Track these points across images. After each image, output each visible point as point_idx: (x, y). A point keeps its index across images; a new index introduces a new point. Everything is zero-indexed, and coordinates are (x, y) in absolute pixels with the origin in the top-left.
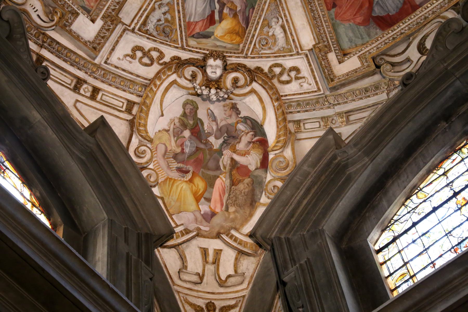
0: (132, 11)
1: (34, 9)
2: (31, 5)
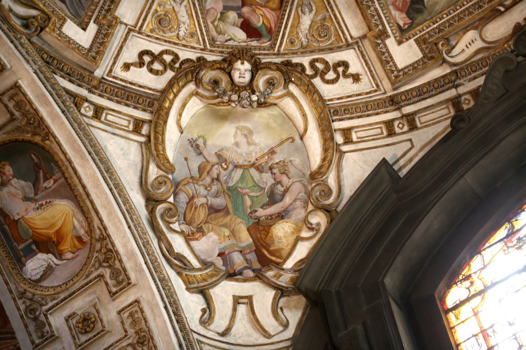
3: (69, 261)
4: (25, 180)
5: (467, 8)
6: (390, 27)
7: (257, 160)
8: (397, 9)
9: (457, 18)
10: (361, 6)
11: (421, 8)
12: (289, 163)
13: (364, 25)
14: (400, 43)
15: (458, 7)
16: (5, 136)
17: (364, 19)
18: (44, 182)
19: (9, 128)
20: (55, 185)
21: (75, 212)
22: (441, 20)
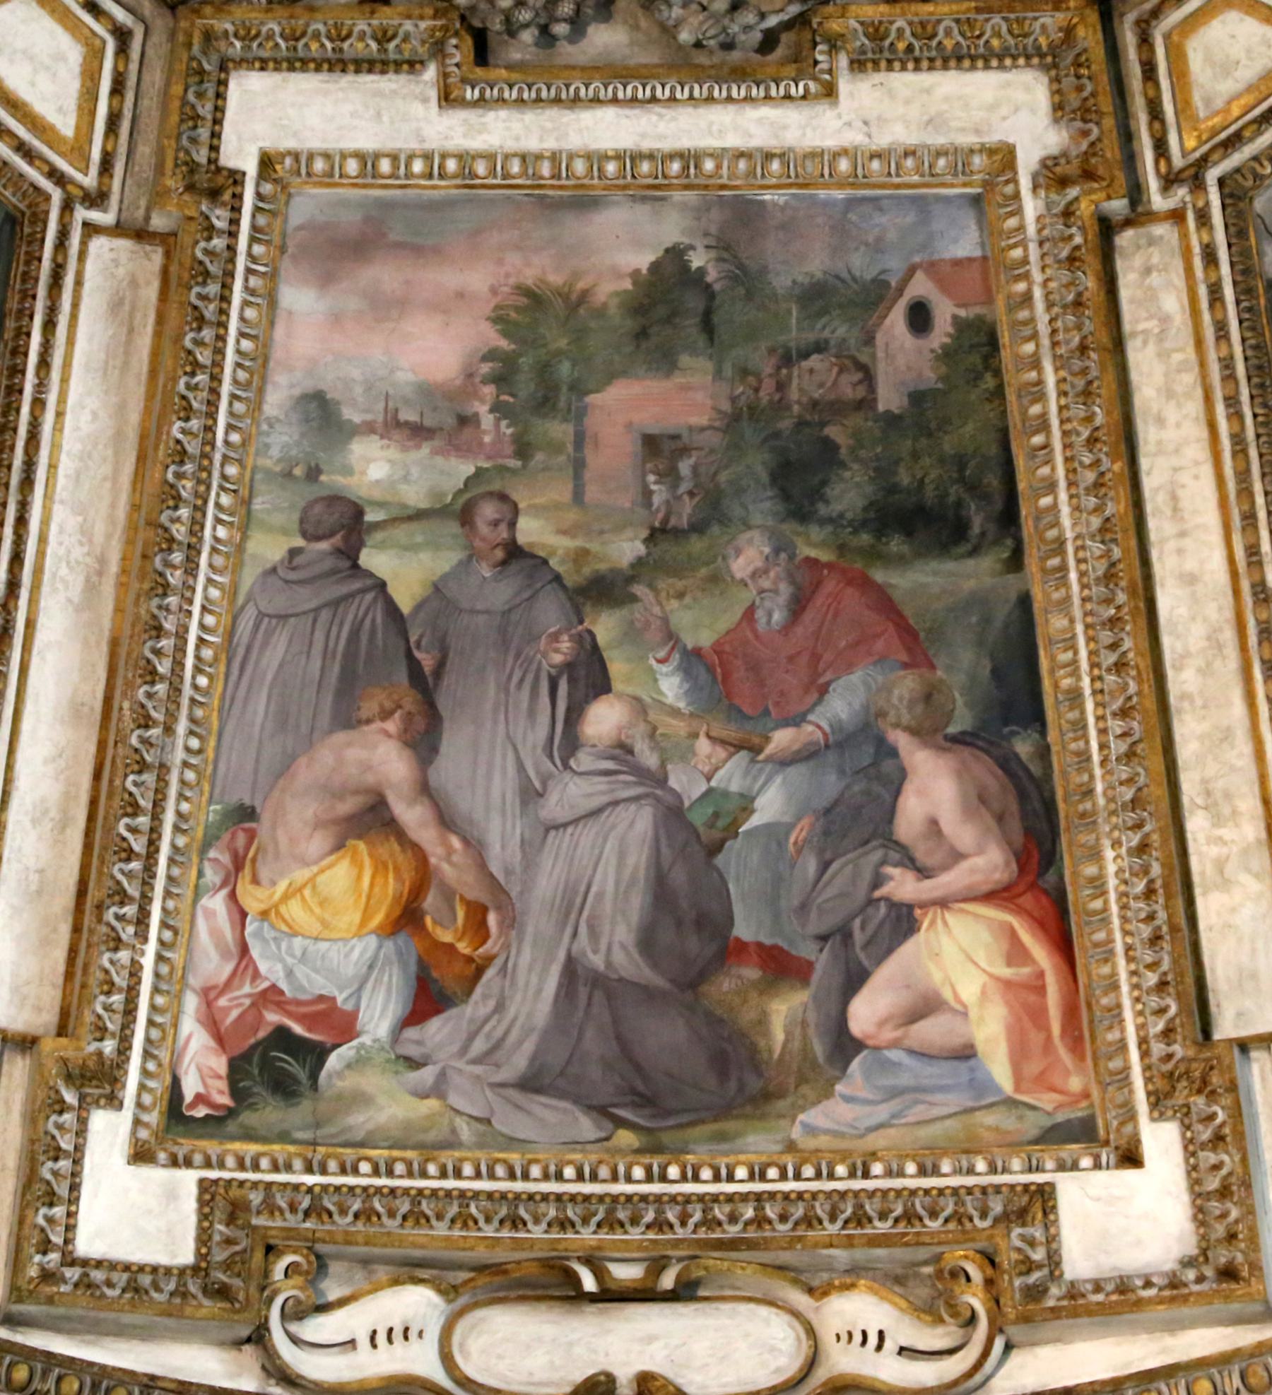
0: (1254, 950)
1: (864, 1342)
2: (844, 1337)
5: (462, 1194)
6: (145, 1072)
8: (211, 1022)
9: (405, 1207)
10: (88, 920)
11: (297, 1081)
13: (51, 998)
14: (141, 1155)
15: (432, 1169)
17: (69, 975)
22: (343, 1171)
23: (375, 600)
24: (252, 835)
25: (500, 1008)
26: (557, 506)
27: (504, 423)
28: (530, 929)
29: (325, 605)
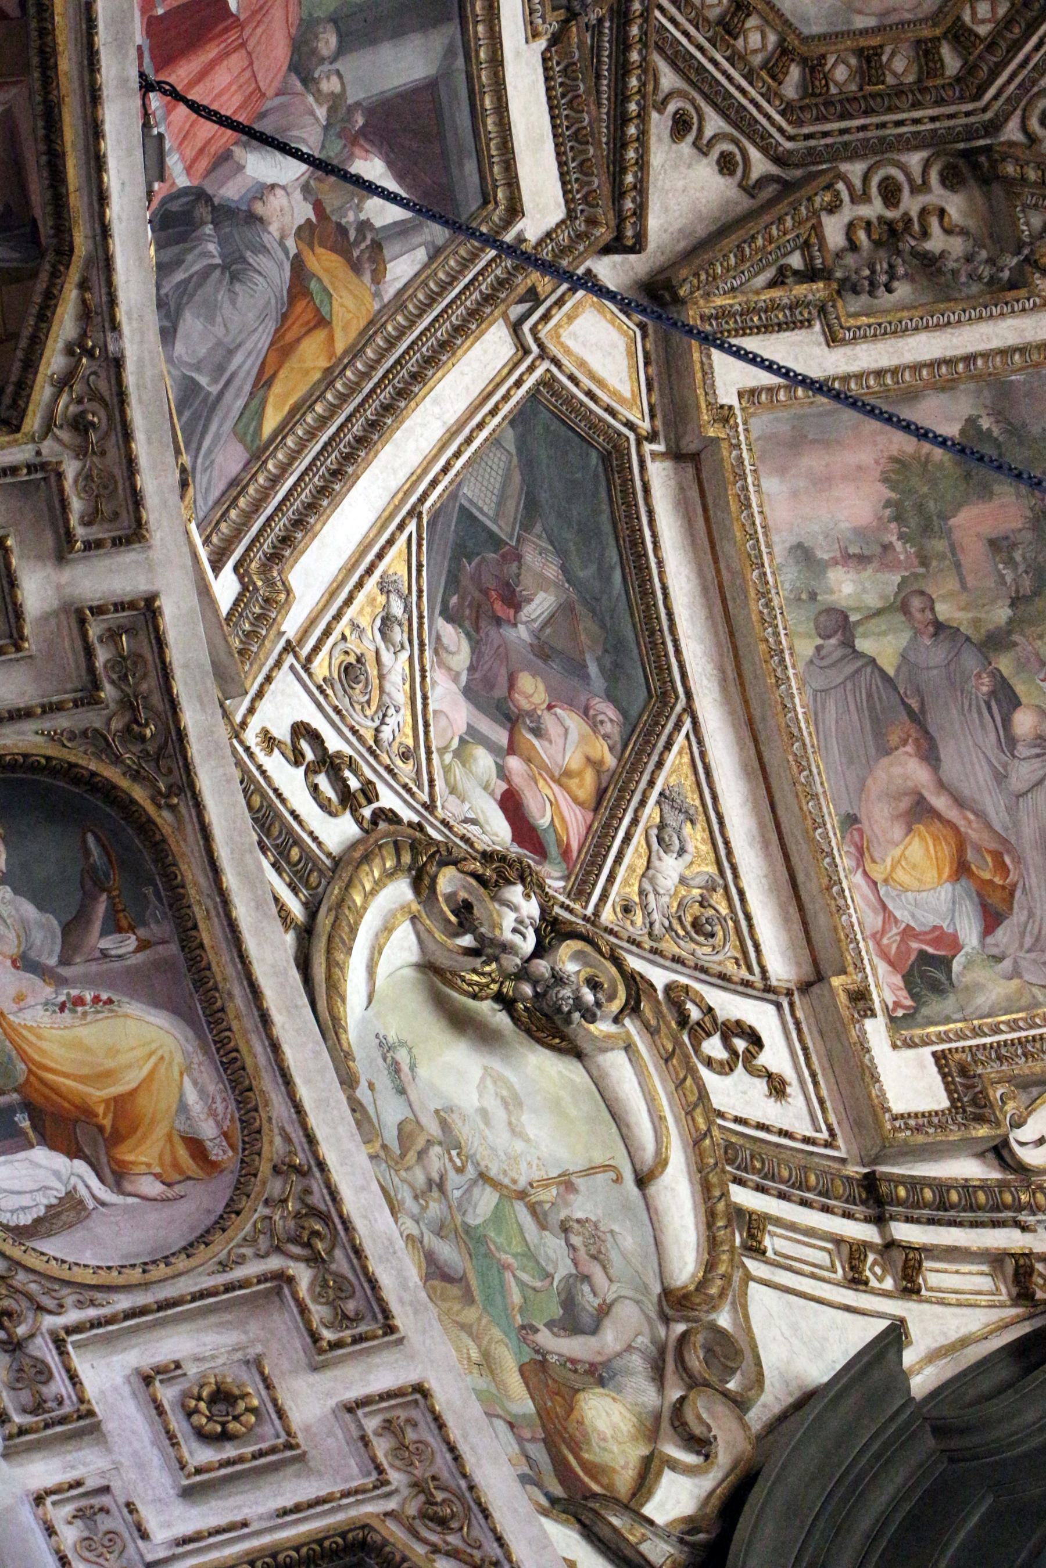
3: (148, 1203)
4: (41, 907)
7: (531, 1185)
8: (884, 955)
11: (942, 984)
12: (609, 1235)
16: (40, 739)
18: (104, 933)
19: (62, 722)
20: (140, 957)
21: (196, 1060)
23: (872, 672)
24: (861, 831)
25: (1031, 915)
26: (951, 594)
27: (908, 545)
28: (1030, 862)
29: (846, 679)
